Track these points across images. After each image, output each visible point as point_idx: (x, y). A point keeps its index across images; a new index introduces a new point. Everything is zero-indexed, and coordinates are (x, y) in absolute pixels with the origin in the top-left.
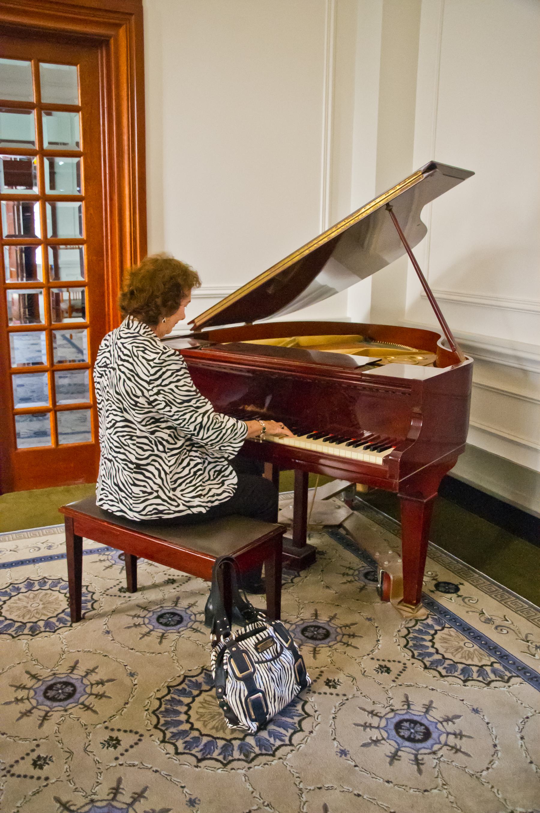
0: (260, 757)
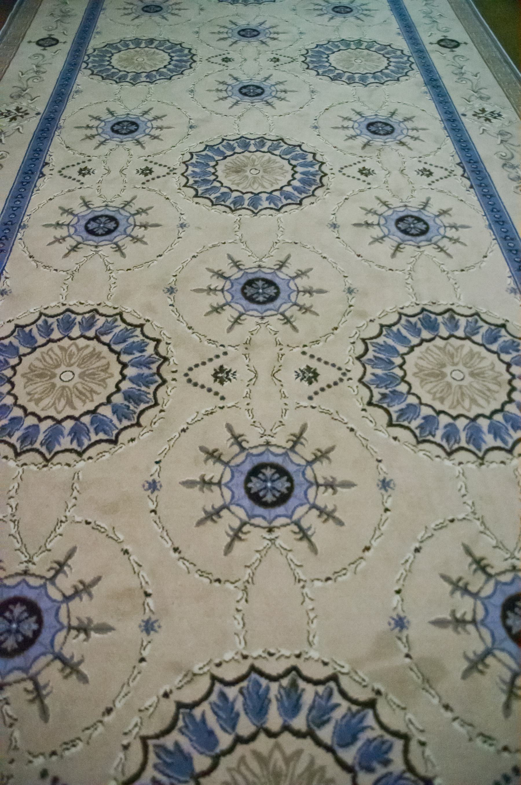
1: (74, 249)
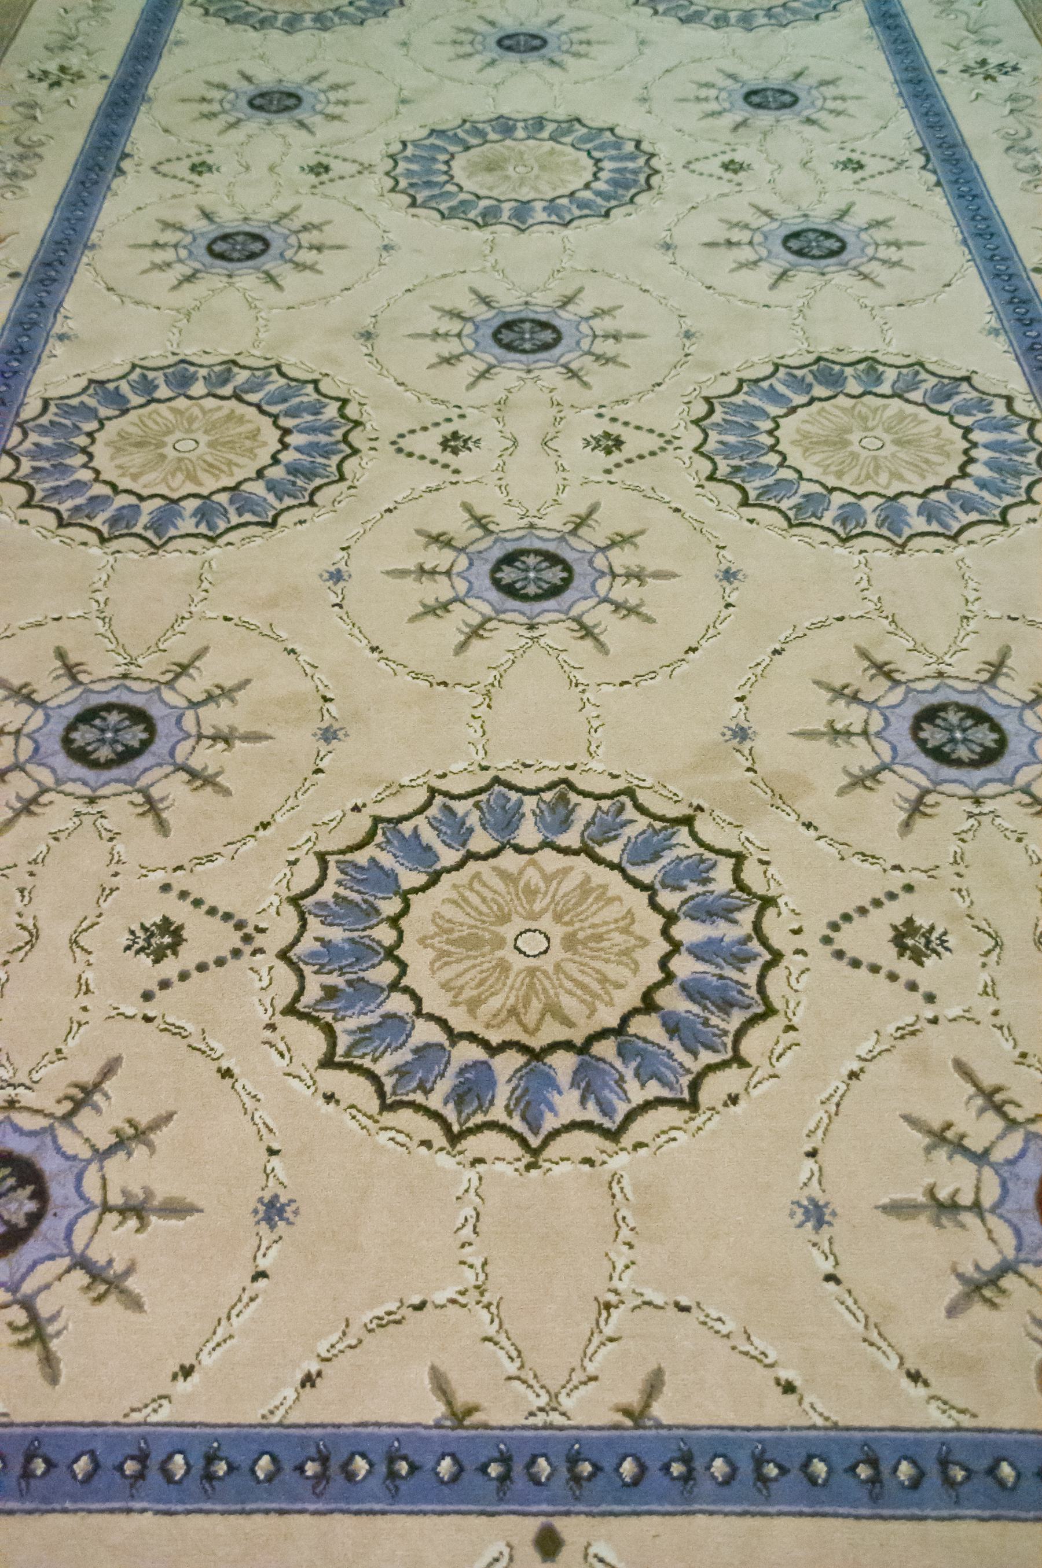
0: (531, 786)
1: (189, 279)
